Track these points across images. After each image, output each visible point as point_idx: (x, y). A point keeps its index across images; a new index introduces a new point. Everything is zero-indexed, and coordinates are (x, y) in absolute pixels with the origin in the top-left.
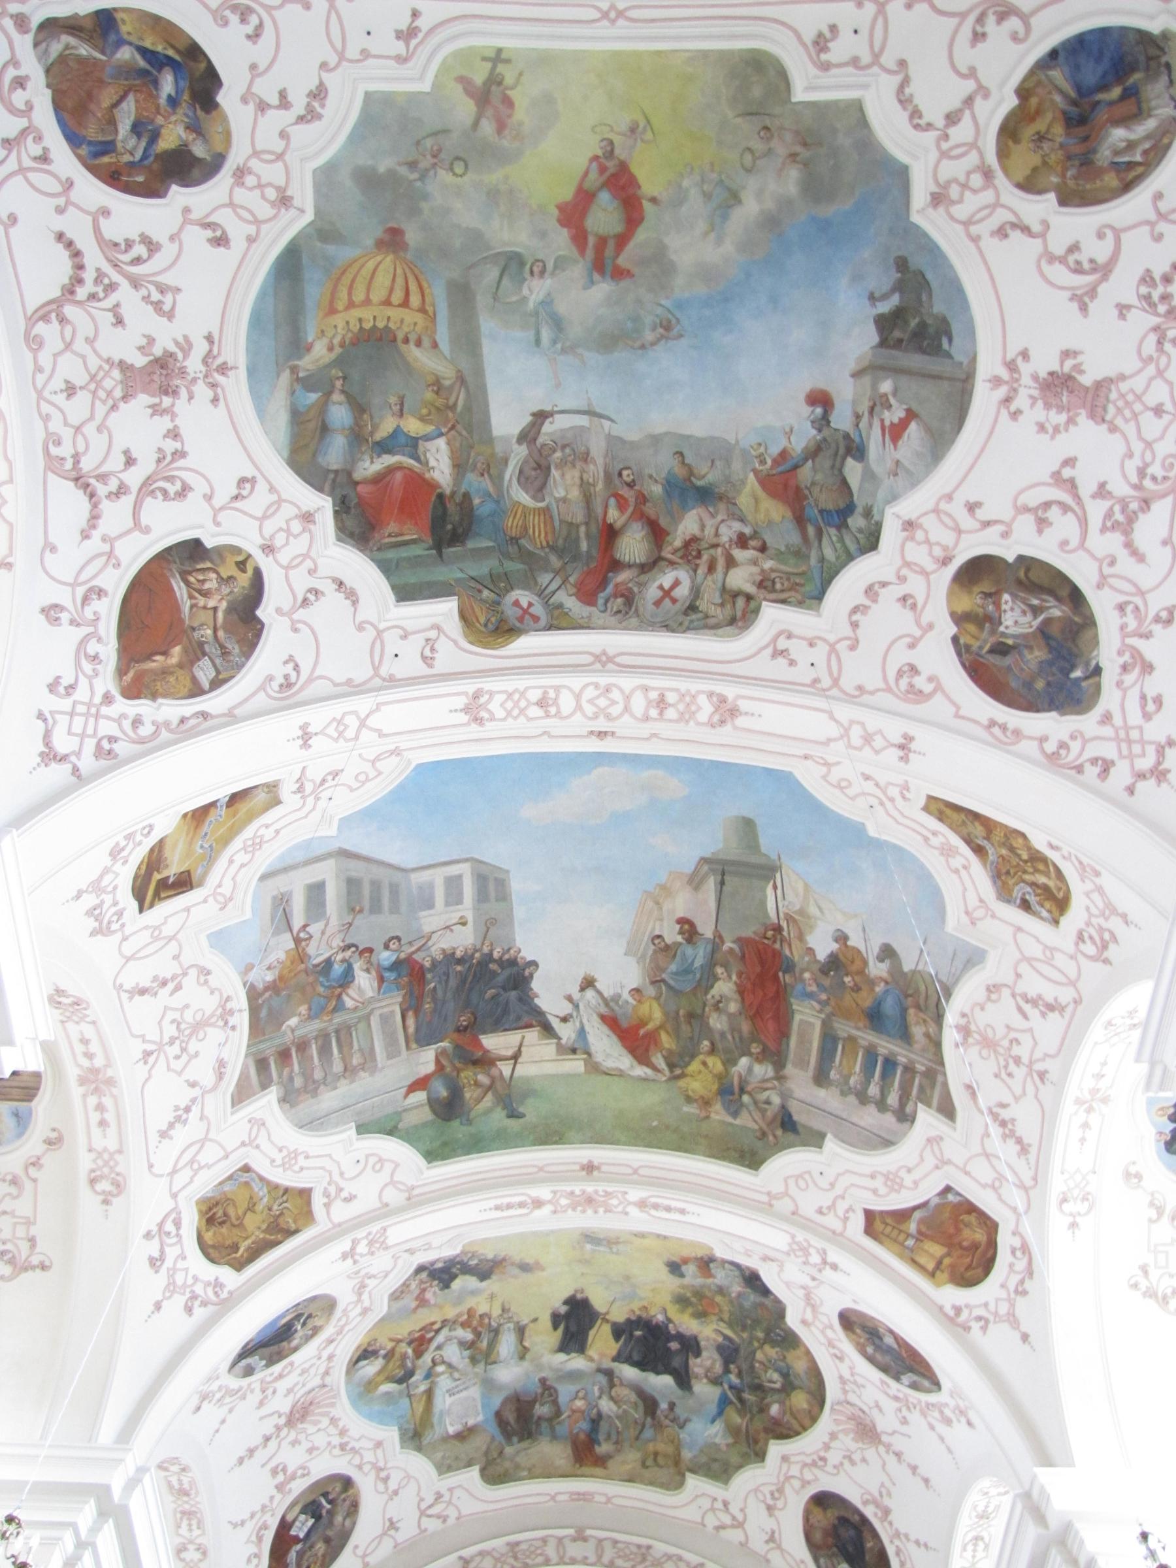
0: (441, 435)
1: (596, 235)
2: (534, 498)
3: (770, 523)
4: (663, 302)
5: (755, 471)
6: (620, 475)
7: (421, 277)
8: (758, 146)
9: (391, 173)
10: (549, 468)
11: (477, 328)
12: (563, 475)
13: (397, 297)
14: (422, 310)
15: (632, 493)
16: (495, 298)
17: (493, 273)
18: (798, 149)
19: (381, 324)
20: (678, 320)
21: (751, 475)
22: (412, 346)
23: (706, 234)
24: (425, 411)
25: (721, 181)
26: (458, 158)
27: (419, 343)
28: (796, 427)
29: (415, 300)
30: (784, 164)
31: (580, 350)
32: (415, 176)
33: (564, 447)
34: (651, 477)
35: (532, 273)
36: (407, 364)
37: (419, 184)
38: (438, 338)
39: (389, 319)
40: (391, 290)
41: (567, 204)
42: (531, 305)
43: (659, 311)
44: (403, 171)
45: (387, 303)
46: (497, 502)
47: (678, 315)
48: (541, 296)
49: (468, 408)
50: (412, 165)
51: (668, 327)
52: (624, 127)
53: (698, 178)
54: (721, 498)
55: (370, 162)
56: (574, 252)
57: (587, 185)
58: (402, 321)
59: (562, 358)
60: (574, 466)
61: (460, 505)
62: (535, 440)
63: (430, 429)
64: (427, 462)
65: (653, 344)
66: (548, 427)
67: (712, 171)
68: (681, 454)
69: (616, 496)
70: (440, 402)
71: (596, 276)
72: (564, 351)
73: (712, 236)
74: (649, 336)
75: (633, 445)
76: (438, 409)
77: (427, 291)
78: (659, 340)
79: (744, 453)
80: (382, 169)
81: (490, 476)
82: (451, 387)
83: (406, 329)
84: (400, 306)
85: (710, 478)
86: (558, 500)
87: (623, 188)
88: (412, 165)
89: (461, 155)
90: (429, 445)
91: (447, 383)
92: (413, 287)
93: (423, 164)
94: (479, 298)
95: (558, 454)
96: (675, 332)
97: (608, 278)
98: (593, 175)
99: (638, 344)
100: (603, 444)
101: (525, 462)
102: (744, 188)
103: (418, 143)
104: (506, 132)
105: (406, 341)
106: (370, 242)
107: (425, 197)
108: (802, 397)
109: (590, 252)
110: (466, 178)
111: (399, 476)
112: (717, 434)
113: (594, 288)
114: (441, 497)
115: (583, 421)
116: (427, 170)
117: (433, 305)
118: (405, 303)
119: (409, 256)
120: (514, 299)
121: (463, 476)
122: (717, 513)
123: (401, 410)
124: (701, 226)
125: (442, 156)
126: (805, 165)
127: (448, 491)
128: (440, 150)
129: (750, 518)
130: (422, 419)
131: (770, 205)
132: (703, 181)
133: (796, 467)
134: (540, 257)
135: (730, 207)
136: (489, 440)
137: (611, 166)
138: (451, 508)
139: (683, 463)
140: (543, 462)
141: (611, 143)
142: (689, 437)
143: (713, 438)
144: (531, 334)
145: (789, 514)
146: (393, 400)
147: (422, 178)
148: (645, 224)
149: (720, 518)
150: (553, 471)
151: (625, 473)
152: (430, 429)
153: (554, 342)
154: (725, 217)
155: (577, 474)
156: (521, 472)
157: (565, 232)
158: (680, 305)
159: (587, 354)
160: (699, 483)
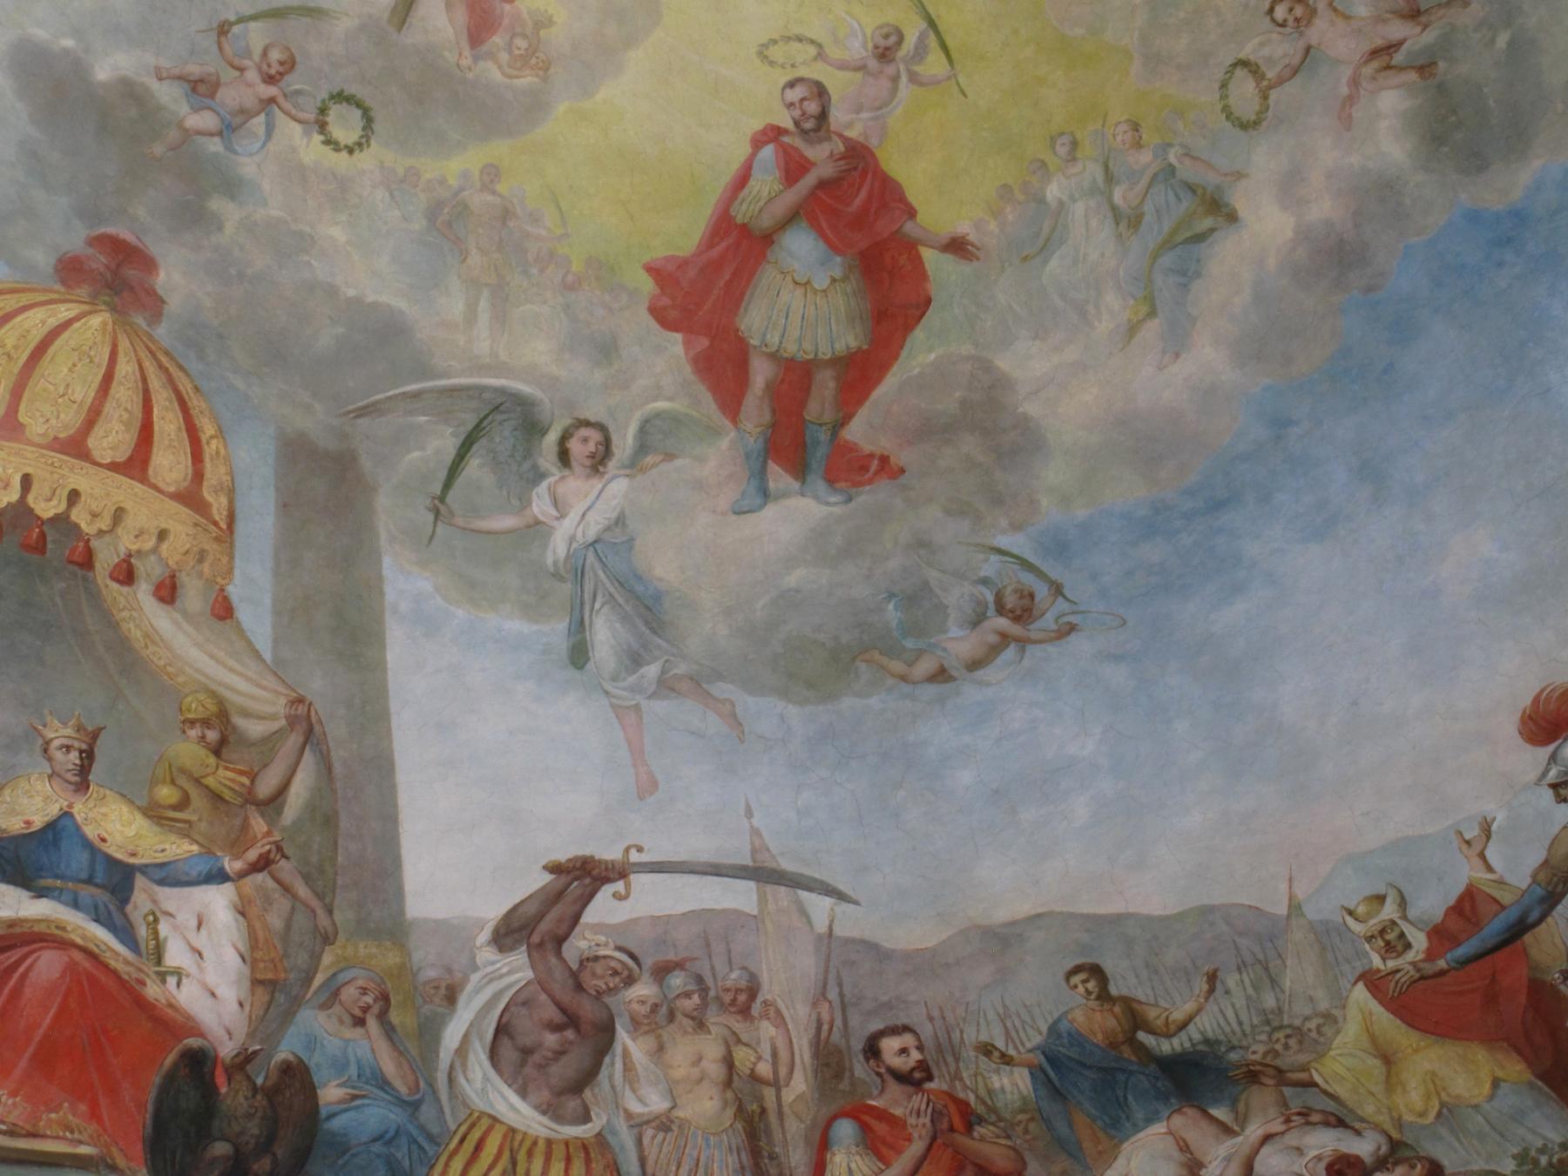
0: (218, 877)
1: (774, 357)
2: (550, 1110)
3: (1448, 1113)
4: (1003, 541)
5: (1374, 982)
6: (872, 1050)
7: (195, 403)
8: (1276, 50)
9: (130, 91)
10: (606, 1032)
11: (376, 585)
12: (661, 1048)
13: (112, 439)
14: (190, 497)
15: (918, 1101)
16: (439, 508)
17: (445, 443)
18: (1397, 30)
19: (46, 509)
20: (1057, 590)
21: (1360, 993)
22: (143, 592)
23: (1132, 329)
24: (166, 793)
25: (1171, 170)
26: (341, 97)
27: (168, 592)
28: (1500, 820)
29: (169, 464)
30: (1355, 82)
31: (722, 690)
32: (206, 120)
33: (662, 972)
34: (987, 1050)
35: (564, 457)
36: (122, 648)
37: (215, 146)
38: (233, 591)
39: (74, 496)
40: (90, 423)
41: (683, 264)
42: (558, 547)
43: (991, 567)
44: (169, 96)
45: (75, 447)
46: (414, 1106)
47: (1055, 573)
48: (595, 524)
49: (324, 816)
50: (201, 88)
51: (1024, 612)
52: (857, 49)
53: (1095, 171)
54: (1253, 1076)
55: (68, 43)
56: (708, 406)
57: (742, 212)
58: (119, 515)
59: (660, 707)
60: (701, 1025)
61: (272, 1093)
62: (560, 940)
63: (177, 848)
64: (159, 958)
65: (974, 665)
66: (604, 909)
67: (1138, 145)
68: (1096, 971)
69: (860, 1114)
70: (223, 778)
71: (779, 477)
72: (666, 687)
73: (1152, 328)
74: (959, 642)
75: (922, 964)
76: (216, 797)
77: (210, 448)
78: (994, 651)
79: (1325, 936)
80: (102, 73)
81: (389, 1031)
82: (270, 743)
83: (126, 542)
84: (114, 467)
85: (1207, 1024)
86: (638, 1124)
87: (860, 221)
88: (201, 88)
89: (353, 89)
90: (169, 897)
91: (255, 729)
92: (167, 424)
93: (231, 96)
94: (383, 501)
95: (643, 990)
96: (1048, 621)
97: (821, 486)
98: (765, 182)
99: (925, 666)
100: (807, 963)
101: (521, 1001)
102: (1239, 175)
103: (223, 30)
104: (498, 40)
105: (126, 574)
106: (42, 259)
107: (232, 187)
108: (1508, 726)
109: (756, 410)
110: (365, 160)
111: (47, 966)
112: (1217, 896)
113: (771, 511)
114: (198, 1062)
115: (740, 896)
116: (246, 114)
117: (231, 493)
118: (136, 464)
119: (161, 332)
120: (507, 522)
121: (288, 1016)
122: (1243, 1120)
123: (84, 770)
124: (1114, 307)
125: (294, 82)
126: (1425, 69)
127: (227, 1050)
128: (289, 65)
129: (1368, 1110)
130: (154, 813)
131: (1324, 208)
132: (1110, 178)
133: (1520, 929)
134: (593, 412)
135: (1200, 238)
136: (395, 930)
137: (822, 157)
138: (232, 1096)
139: (1104, 996)
140: (587, 1009)
141: (820, 92)
142: (1117, 920)
143: (1206, 911)
144: (556, 631)
145: (1516, 1069)
146: (59, 733)
147: (228, 130)
148: (932, 317)
149: (1254, 1131)
150: (623, 1035)
151: (890, 1045)
152: (177, 848)
153: (635, 660)
154: (1187, 275)
155: (712, 1050)
156: (502, 1030)
157: (675, 343)
158: (1059, 547)
159: (749, 704)
160: (1166, 1047)
